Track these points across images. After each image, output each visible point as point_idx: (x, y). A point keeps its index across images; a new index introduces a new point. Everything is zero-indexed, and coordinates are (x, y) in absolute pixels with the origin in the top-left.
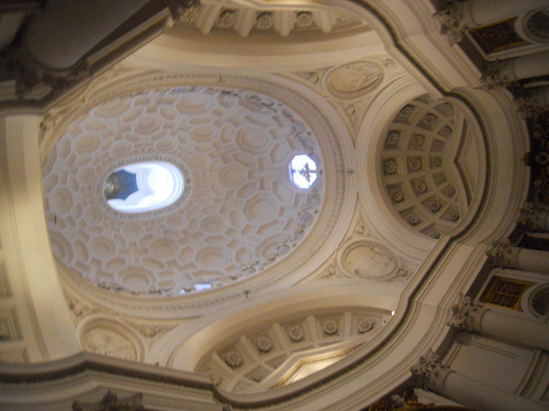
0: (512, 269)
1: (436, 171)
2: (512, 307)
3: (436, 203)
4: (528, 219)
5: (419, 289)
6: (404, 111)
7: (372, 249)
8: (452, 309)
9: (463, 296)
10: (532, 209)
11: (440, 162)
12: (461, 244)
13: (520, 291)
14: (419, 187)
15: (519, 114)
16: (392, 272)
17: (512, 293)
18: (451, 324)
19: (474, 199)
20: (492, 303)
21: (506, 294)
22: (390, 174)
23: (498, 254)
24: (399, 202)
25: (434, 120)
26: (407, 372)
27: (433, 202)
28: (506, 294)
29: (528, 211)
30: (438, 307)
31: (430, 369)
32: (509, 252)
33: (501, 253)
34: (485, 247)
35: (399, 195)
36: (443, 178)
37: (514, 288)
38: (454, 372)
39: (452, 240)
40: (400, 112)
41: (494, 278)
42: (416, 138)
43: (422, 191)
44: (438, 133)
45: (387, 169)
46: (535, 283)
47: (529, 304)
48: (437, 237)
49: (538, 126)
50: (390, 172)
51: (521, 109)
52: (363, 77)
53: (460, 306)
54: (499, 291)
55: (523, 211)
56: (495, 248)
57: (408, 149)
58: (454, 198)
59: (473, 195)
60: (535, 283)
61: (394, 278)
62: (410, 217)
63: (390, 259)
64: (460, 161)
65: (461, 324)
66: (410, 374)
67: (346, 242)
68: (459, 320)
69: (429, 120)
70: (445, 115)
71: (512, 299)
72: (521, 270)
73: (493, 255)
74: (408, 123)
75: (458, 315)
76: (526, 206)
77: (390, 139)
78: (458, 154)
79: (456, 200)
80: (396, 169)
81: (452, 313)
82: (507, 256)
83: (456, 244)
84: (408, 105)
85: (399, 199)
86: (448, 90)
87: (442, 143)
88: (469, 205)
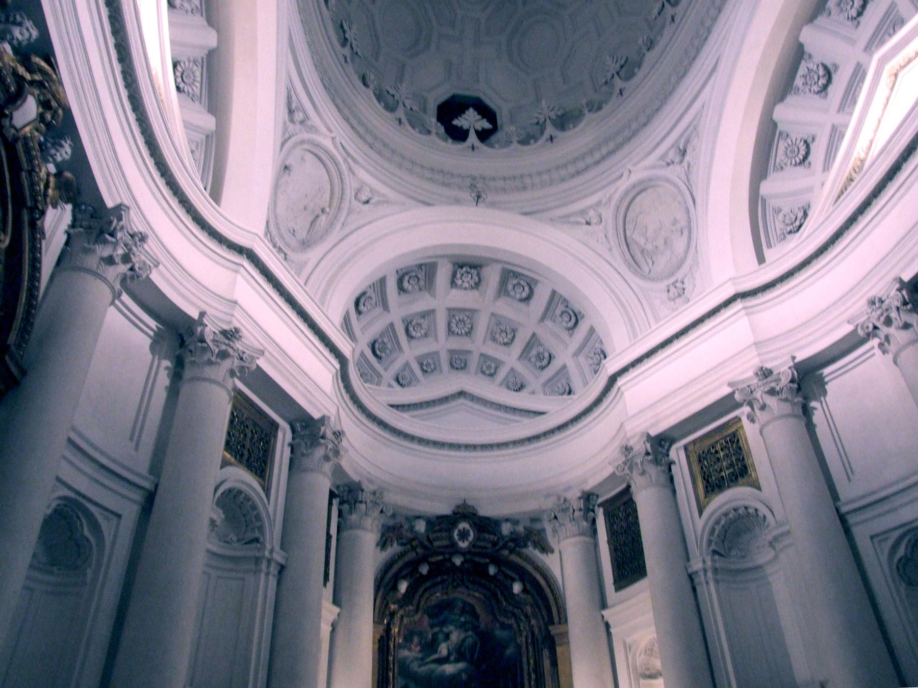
3: (388, 351)
5: (262, 274)
6: (569, 314)
12: (333, 377)
22: (454, 275)
25: (539, 364)
27: (389, 346)
28: (248, 445)
30: (235, 302)
36: (429, 370)
42: (509, 331)
43: (411, 329)
44: (512, 369)
45: (464, 269)
50: (458, 276)
52: (649, 247)
53: (238, 345)
54: (252, 431)
56: (331, 435)
57: (493, 314)
58: (394, 384)
59: (405, 415)
62: (370, 298)
64: (461, 400)
65: (203, 340)
67: (345, 160)
68: (211, 337)
70: (545, 384)
74: (543, 319)
75: (221, 338)
77: (519, 284)
78: (473, 398)
79: (390, 386)
80: (461, 287)
81: (226, 327)
85: (406, 284)
88: (392, 406)
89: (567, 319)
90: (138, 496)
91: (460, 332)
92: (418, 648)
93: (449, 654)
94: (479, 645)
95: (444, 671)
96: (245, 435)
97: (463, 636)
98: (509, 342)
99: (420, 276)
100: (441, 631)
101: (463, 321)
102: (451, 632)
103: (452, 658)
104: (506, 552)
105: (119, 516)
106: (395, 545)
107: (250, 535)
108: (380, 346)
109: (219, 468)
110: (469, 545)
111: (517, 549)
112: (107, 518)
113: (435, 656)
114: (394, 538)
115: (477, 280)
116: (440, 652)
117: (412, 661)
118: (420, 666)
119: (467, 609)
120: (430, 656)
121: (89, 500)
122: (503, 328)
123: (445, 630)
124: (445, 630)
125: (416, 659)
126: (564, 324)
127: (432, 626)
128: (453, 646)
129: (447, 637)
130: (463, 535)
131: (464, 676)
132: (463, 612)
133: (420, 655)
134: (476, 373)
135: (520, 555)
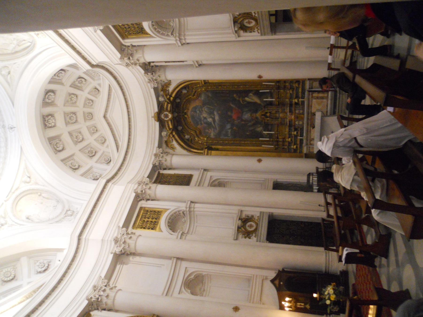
0: (152, 200)
1: (89, 123)
2: (155, 230)
3: (92, 149)
4: (160, 161)
7: (40, 195)
8: (114, 240)
9: (121, 228)
11: (92, 116)
13: (159, 216)
14: (76, 137)
15: (149, 84)
16: (61, 213)
17: (154, 218)
18: (114, 252)
19: (121, 147)
20: (141, 228)
21: (150, 220)
22: (50, 127)
23: (142, 191)
24: (60, 151)
25: (84, 82)
26: (83, 301)
27: (89, 149)
28: (150, 220)
29: (160, 155)
30: (102, 240)
31: (102, 293)
32: (150, 188)
33: (144, 190)
34: (133, 185)
35: (60, 145)
36: (96, 129)
37: (155, 215)
38: (120, 290)
39: (108, 181)
40: (55, 75)
41: (141, 208)
43: (79, 140)
44: (89, 93)
46: (168, 209)
47: (165, 225)
48: (96, 179)
50: (50, 125)
51: (150, 81)
53: (119, 236)
54: (145, 218)
55: (156, 155)
56: (140, 186)
57: (64, 105)
59: (120, 144)
60: (168, 209)
61: (63, 218)
62: (71, 164)
63: (58, 202)
64: (108, 116)
65: (121, 251)
66: (86, 302)
68: (119, 248)
69: (80, 82)
70: (94, 79)
71: (154, 223)
72: (158, 200)
73: (139, 192)
74: (62, 84)
75: (118, 244)
76: (158, 151)
77: (48, 98)
78: (106, 111)
79: (107, 146)
81: (113, 243)
82: (148, 192)
83: (111, 185)
84: (62, 70)
85: (61, 148)
86: (95, 64)
87: (92, 101)
88: (118, 151)
89: (61, 74)
90: (179, 262)
91: (76, 118)
92: (210, 130)
93: (211, 117)
96: (148, 221)
97: (204, 112)
98: (76, 96)
99: (55, 143)
101: (70, 118)
102: (203, 117)
103: (213, 116)
104: (172, 98)
105: (186, 268)
107: (182, 214)
108: (91, 153)
109: (162, 233)
110: (170, 113)
111: (170, 94)
112: (188, 271)
114: (170, 144)
115: (50, 116)
118: (216, 129)
120: (212, 125)
121: (183, 279)
122: (70, 100)
123: (203, 119)
124: (203, 119)
125: (214, 131)
126: (63, 75)
127: (201, 124)
129: (205, 118)
130: (166, 116)
131: (219, 112)
132: (195, 112)
134: (93, 108)
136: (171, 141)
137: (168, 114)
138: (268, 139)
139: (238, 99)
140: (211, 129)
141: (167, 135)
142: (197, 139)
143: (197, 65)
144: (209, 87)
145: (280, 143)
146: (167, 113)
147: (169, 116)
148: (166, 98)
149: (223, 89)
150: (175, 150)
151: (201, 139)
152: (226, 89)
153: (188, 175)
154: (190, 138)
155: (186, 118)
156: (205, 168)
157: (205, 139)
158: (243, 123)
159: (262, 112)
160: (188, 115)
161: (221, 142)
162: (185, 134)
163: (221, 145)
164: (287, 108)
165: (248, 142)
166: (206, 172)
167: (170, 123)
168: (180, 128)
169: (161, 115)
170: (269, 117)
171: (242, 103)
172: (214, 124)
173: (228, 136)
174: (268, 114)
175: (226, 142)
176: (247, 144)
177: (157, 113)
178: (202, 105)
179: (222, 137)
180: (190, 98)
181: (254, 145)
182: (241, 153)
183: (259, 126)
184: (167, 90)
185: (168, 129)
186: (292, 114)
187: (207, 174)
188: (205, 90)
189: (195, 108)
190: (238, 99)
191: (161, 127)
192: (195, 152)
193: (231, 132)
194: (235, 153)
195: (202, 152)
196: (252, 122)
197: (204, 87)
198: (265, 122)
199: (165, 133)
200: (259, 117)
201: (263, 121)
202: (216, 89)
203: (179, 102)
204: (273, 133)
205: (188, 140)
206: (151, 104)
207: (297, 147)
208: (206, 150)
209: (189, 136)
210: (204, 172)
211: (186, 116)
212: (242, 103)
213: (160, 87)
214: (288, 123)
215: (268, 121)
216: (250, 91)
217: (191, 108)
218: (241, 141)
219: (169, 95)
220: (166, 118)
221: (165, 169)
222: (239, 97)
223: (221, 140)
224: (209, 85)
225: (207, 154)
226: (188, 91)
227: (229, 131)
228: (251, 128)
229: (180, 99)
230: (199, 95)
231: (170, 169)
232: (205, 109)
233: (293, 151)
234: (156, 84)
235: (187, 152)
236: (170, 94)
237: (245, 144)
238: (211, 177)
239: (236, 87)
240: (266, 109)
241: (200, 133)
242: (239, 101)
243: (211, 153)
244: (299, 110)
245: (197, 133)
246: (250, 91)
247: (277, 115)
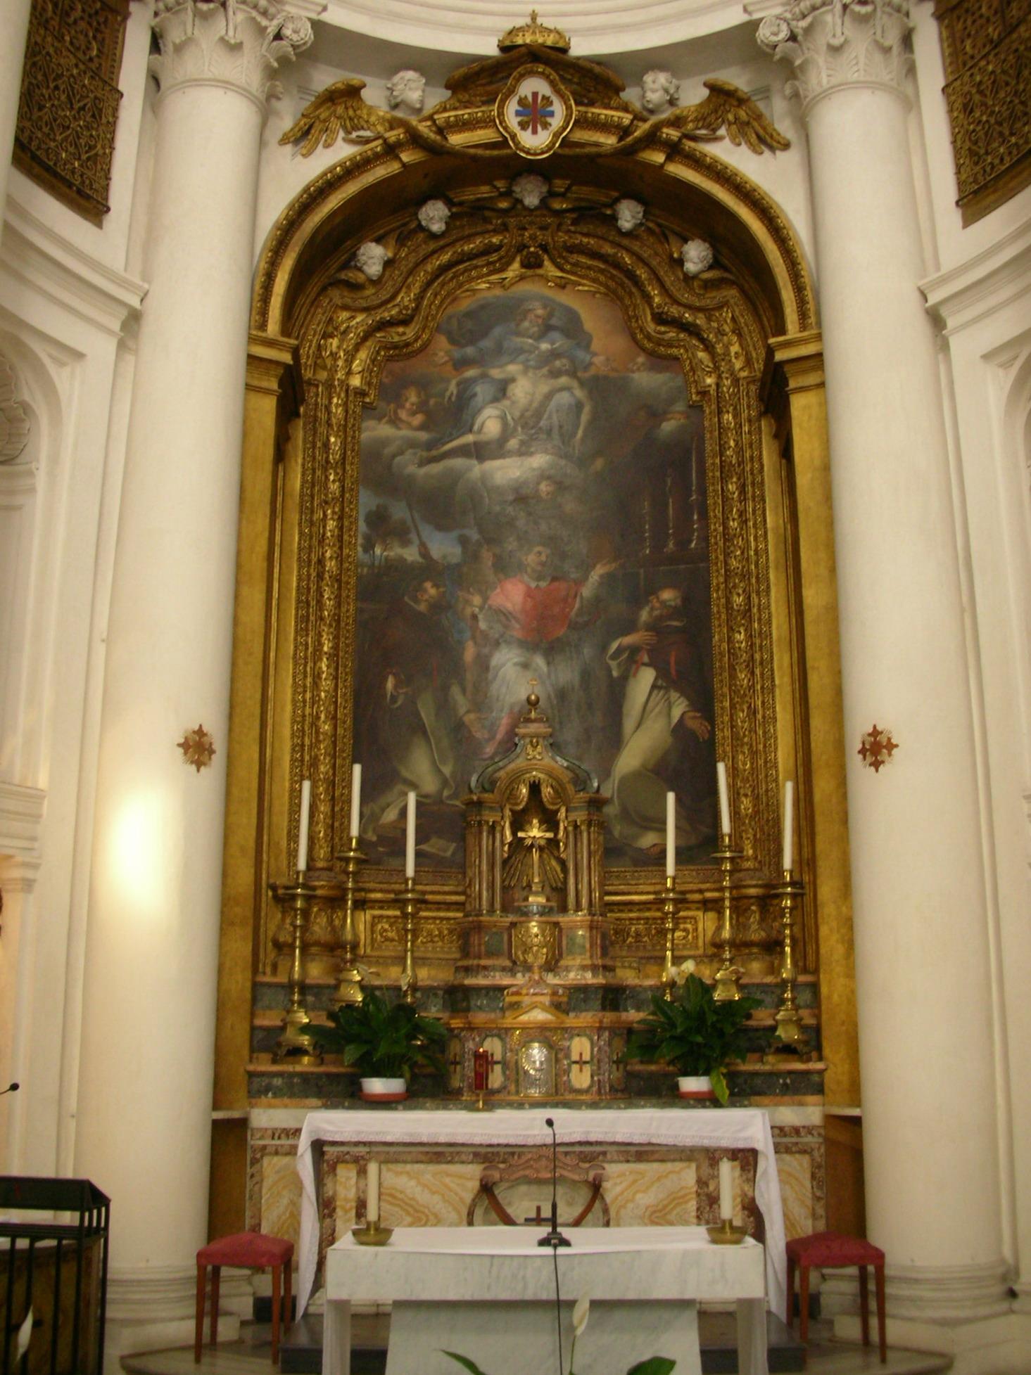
10: (278, 37)
29: (265, 13)
49: (693, 95)
92: (418, 419)
94: (587, 410)
95: (484, 478)
97: (544, 388)
100: (484, 376)
102: (513, 380)
104: (659, 158)
106: (339, 141)
111: (689, 144)
113: (470, 438)
114: (335, 124)
116: (480, 431)
117: (401, 453)
119: (554, 321)
123: (496, 373)
124: (496, 373)
125: (412, 444)
127: (461, 364)
128: (517, 414)
129: (502, 389)
130: (534, 115)
132: (546, 329)
133: (423, 436)
135: (698, 162)
136: (354, 135)
137: (546, 126)
138: (355, 830)
139: (644, 615)
140: (422, 427)
141: (396, 106)
142: (354, 323)
143: (933, 299)
144: (728, 417)
145: (320, 927)
146: (556, 122)
147: (535, 132)
148: (663, 116)
149: (716, 513)
150: (289, 148)
151: (357, 348)
152: (716, 527)
153: (106, 188)
154: (361, 278)
155: (502, 270)
156: (149, 326)
157: (356, 381)
158: (469, 653)
159: (560, 792)
160: (522, 278)
161: (334, 487)
162: (392, 242)
163: (313, 484)
164: (594, 968)
165: (326, 684)
166: (116, 326)
167: (484, 135)
168: (434, 215)
169: (547, 77)
170: (518, 844)
171: (615, 645)
172: (464, 451)
173: (368, 547)
174: (535, 832)
175: (331, 524)
176: (317, 676)
177: (561, 44)
178: (592, 371)
179: (366, 501)
180: (648, 298)
181: (305, 726)
182: (254, 617)
183: (447, 770)
184: (714, 130)
185: (441, 118)
186: (557, 1007)
187: (109, 331)
188: (704, 393)
189: (573, 328)
190: (644, 615)
191: (463, 71)
192: (270, 277)
193: (402, 560)
194: (257, 562)
195: (273, 328)
196: (470, 718)
197: (727, 383)
198: (479, 804)
199: (414, 96)
200: (520, 763)
201: (487, 796)
202: (712, 461)
203: (614, 218)
204: (410, 871)
205: (351, 261)
206: (626, 18)
207: (297, 1052)
208: (287, 358)
209: (374, 269)
210: (123, 313)
211: (516, 265)
212: (615, 645)
213: (737, 79)
214: (480, 981)
215: (492, 830)
216: (704, 703)
217: (565, 298)
218: (338, 627)
219: (680, 139)
220: (518, 113)
221: (156, 45)
222: (655, 627)
223: (342, 481)
224: (745, 415)
225: (252, 360)
226: (688, 279)
227: (411, 554)
228: (426, 711)
229: (629, 234)
230: (660, 359)
231: (154, 80)
232: (568, 394)
233: (269, 1019)
234: (784, 34)
235: (278, 227)
236: (689, 144)
237: (317, 658)
238: (79, 356)
239: (738, 600)
240: (580, 816)
241: (395, 346)
242: (630, 627)
243: (267, 392)
244: (596, 1061)
245: (401, 330)
246: (704, 703)
247: (536, 900)
